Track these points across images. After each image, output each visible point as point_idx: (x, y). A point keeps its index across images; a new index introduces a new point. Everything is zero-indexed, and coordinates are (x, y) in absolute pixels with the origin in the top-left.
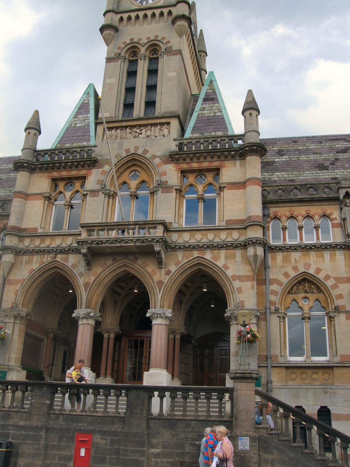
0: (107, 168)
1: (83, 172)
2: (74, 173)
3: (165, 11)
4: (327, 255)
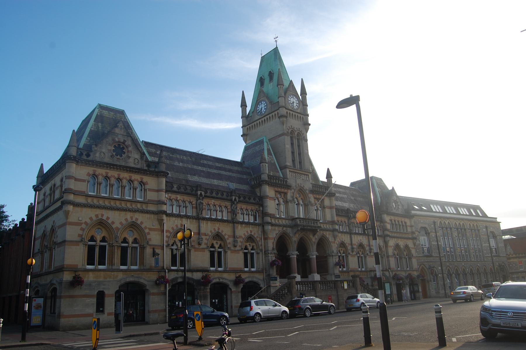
0: (293, 190)
1: (286, 191)
2: (283, 190)
3: (302, 116)
4: (346, 235)
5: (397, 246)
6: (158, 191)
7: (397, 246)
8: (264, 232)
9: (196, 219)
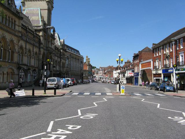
5: (63, 62)
6: (19, 26)
7: (63, 62)
8: (40, 51)
9: (25, 41)
